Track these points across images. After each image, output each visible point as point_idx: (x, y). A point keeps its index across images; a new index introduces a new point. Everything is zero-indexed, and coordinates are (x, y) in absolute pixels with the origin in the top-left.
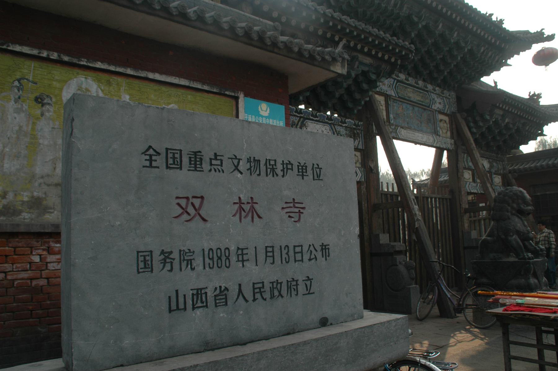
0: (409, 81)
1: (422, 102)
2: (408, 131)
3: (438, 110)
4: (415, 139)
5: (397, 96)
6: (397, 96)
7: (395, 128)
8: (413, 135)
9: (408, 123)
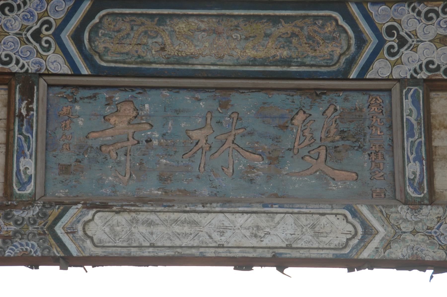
1: (287, 62)
2: (142, 217)
3: (424, 75)
4: (198, 247)
5: (85, 70)
6: (85, 70)
7: (45, 215)
8: (186, 229)
9: (162, 178)
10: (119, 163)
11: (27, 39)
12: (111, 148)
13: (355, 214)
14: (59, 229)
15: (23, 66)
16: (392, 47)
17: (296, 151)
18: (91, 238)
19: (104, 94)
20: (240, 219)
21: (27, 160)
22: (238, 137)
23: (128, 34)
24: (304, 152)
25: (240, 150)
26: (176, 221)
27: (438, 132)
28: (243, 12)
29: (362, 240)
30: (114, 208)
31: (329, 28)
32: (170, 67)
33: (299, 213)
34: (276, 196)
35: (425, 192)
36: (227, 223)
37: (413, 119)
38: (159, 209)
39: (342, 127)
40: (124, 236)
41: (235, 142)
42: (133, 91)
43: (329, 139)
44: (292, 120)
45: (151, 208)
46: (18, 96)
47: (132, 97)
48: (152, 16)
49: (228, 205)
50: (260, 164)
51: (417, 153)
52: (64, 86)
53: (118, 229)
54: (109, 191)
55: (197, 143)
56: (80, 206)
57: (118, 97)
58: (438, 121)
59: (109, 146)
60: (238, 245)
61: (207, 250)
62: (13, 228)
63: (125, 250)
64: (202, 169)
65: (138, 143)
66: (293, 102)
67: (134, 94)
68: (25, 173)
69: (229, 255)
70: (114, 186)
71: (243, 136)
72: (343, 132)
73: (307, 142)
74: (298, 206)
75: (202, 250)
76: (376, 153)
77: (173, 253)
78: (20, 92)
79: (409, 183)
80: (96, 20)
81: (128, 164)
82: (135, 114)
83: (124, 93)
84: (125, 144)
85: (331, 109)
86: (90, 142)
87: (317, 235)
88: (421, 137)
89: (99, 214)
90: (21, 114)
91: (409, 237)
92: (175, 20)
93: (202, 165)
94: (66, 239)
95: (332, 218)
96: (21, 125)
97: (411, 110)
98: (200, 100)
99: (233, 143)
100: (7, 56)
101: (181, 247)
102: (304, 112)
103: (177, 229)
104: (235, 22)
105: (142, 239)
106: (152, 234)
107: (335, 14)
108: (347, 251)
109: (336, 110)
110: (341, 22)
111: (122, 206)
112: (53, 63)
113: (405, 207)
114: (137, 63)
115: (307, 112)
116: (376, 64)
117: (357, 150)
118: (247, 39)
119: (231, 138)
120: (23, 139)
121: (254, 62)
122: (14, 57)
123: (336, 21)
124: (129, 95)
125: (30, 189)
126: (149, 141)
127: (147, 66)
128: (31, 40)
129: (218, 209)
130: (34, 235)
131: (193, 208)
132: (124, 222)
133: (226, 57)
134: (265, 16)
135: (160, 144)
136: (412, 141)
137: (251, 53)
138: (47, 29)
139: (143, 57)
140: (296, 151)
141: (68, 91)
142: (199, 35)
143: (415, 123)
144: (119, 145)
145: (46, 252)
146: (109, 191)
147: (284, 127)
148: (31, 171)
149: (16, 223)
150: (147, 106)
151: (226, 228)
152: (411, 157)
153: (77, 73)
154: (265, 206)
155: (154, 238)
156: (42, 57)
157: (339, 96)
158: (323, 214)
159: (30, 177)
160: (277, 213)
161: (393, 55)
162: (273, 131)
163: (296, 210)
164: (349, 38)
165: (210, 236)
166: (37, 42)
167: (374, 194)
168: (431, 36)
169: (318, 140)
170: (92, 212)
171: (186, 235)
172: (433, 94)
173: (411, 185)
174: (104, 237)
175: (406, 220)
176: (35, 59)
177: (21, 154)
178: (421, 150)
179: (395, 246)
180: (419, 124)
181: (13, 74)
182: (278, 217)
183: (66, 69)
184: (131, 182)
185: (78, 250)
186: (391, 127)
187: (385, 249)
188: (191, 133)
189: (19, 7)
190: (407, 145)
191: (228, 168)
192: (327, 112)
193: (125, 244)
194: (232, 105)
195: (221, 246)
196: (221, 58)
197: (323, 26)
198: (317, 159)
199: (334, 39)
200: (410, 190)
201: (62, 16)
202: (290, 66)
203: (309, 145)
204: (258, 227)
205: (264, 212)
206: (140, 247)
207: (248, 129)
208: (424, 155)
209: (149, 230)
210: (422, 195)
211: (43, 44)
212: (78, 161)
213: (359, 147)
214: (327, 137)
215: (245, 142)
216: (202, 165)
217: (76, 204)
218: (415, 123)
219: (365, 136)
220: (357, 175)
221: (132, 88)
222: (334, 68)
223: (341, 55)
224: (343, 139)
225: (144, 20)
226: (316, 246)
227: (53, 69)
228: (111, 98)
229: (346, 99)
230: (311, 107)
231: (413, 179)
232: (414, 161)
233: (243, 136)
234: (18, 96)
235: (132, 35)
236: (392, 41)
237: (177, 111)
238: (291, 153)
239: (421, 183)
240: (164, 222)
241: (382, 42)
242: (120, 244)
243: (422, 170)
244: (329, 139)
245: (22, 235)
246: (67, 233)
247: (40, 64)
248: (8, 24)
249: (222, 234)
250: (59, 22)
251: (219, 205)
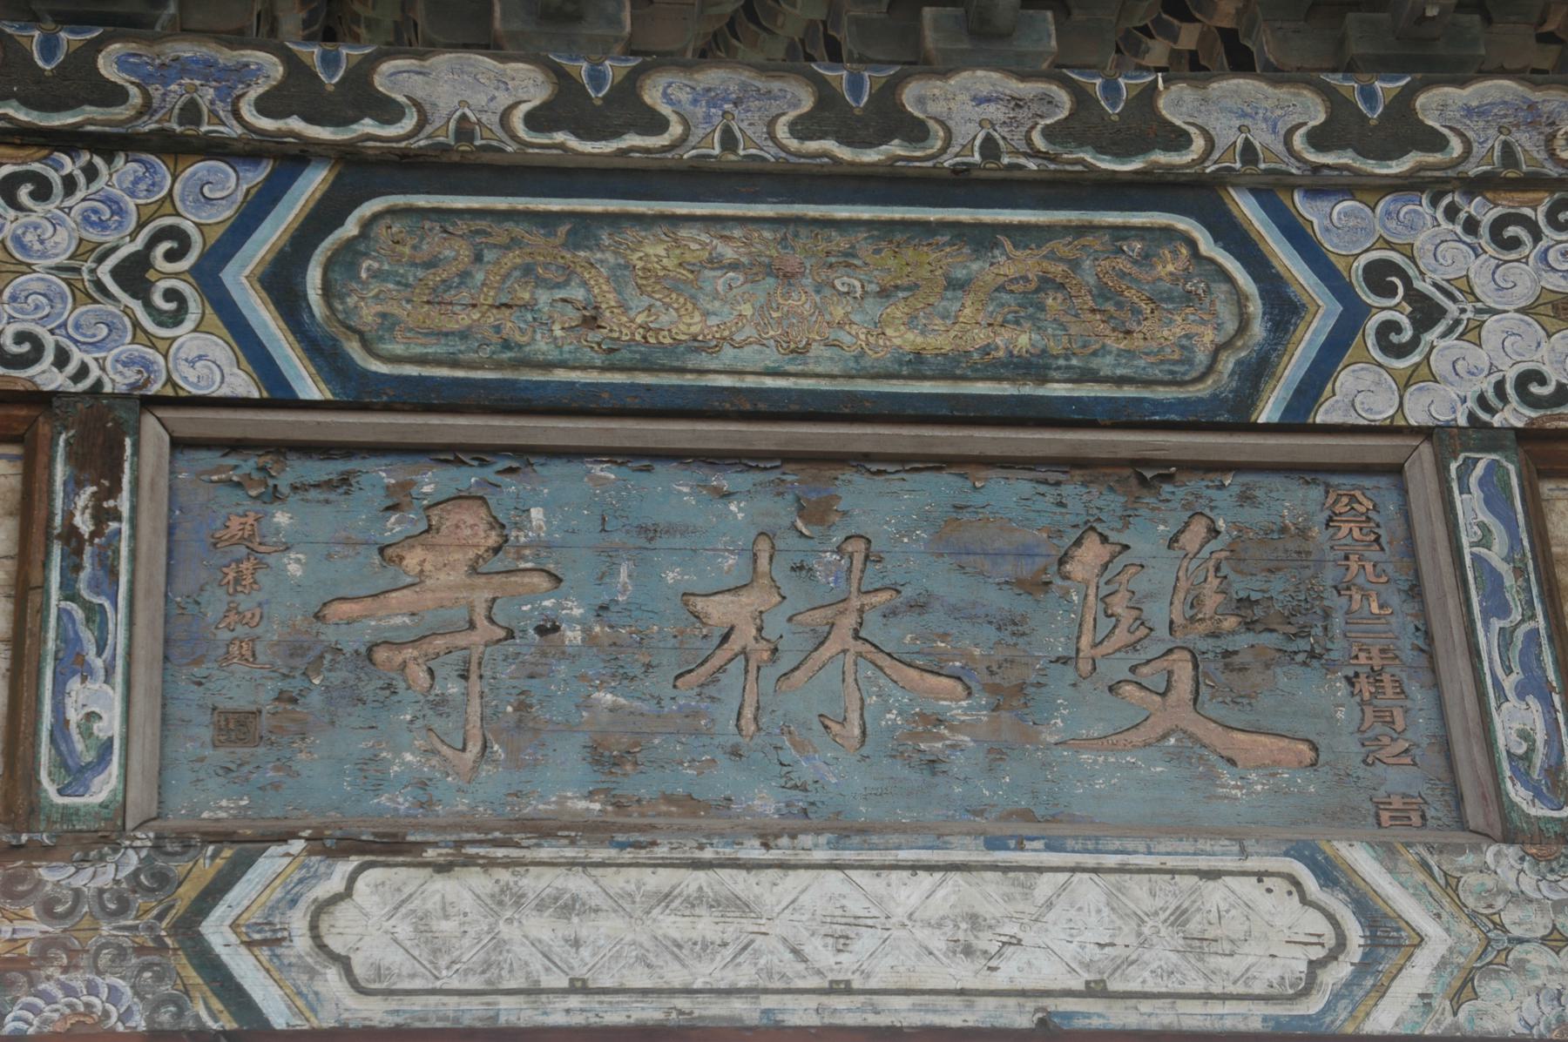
0: (658, 124)
1: (1033, 367)
2: (535, 883)
3: (1514, 415)
4: (753, 992)
5: (309, 387)
6: (309, 387)
7: (163, 880)
8: (706, 926)
10: (440, 704)
11: (100, 286)
12: (409, 652)
13: (1329, 873)
14: (216, 931)
15: (83, 371)
16: (1389, 327)
17: (1085, 667)
18: (344, 963)
19: (381, 474)
20: (903, 893)
21: (96, 685)
22: (870, 617)
23: (465, 275)
24: (1118, 669)
25: (885, 662)
26: (665, 898)
28: (865, 213)
29: (1366, 966)
30: (430, 854)
31: (1169, 266)
33: (1122, 870)
34: (1027, 816)
36: (856, 906)
37: (1495, 556)
38: (599, 854)
39: (1242, 586)
40: (470, 953)
41: (862, 634)
42: (483, 463)
44: (1062, 562)
45: (570, 853)
46: (60, 471)
48: (547, 220)
49: (856, 840)
50: (958, 709)
53: (447, 926)
54: (403, 803)
55: (725, 638)
56: (297, 846)
57: (431, 482)
60: (904, 983)
62: (36, 928)
64: (749, 726)
65: (510, 635)
66: (1061, 504)
67: (489, 473)
68: (87, 733)
69: (873, 1020)
70: (423, 785)
71: (890, 613)
72: (1245, 602)
73: (1121, 637)
74: (1117, 844)
75: (768, 1002)
78: (70, 457)
79: (1514, 769)
80: (350, 228)
81: (475, 708)
82: (493, 539)
83: (453, 471)
84: (461, 640)
85: (1199, 528)
86: (330, 635)
87: (1197, 946)
88: (1533, 617)
90: (71, 532)
91: (1539, 958)
92: (631, 234)
93: (748, 713)
94: (245, 968)
95: (1247, 886)
96: (72, 568)
97: (1483, 526)
98: (727, 496)
99: (857, 637)
100: (20, 338)
101: (688, 991)
102: (1104, 539)
103: (670, 925)
104: (840, 242)
105: (537, 964)
106: (576, 943)
107: (1183, 224)
108: (1312, 1006)
109: (1214, 532)
110: (1207, 245)
111: (459, 844)
112: (192, 363)
113: (1512, 851)
114: (499, 366)
115: (1114, 537)
116: (1346, 380)
117: (1304, 664)
118: (884, 293)
119: (850, 621)
120: (79, 614)
121: (916, 364)
122: (49, 341)
123: (1192, 244)
124: (469, 477)
125: (103, 789)
127: (537, 376)
129: (820, 856)
130: (121, 953)
131: (728, 852)
132: (467, 902)
133: (817, 349)
134: (943, 225)
135: (590, 639)
137: (905, 339)
138: (171, 256)
139: (520, 346)
140: (1085, 667)
141: (248, 464)
142: (720, 281)
143: (1504, 568)
144: (440, 642)
145: (165, 1017)
147: (1037, 586)
148: (111, 725)
149: (48, 911)
150: (536, 514)
151: (856, 922)
152: (1509, 683)
153: (281, 398)
154: (993, 844)
155: (582, 964)
156: (152, 342)
157: (1222, 487)
158: (1212, 875)
159: (106, 748)
160: (1040, 870)
161: (1401, 351)
162: (1000, 600)
163: (1111, 860)
164: (1240, 299)
166: (134, 296)
167: (1385, 816)
168: (1524, 292)
169: (1162, 631)
170: (344, 868)
171: (705, 948)
172: (1547, 488)
173: (1522, 776)
174: (394, 958)
175: (1518, 898)
176: (127, 348)
177: (73, 664)
179: (1489, 988)
180: (1520, 572)
181: (42, 400)
182: (1046, 885)
183: (242, 384)
184: (486, 770)
186: (1415, 591)
187: (1457, 999)
188: (700, 604)
189: (70, 184)
190: (1487, 641)
191: (843, 722)
192: (1183, 538)
193: (474, 983)
194: (845, 513)
196: (800, 352)
197: (1146, 259)
198: (1163, 695)
199: (1189, 298)
201: (227, 213)
202: (1043, 380)
203: (1133, 646)
204: (974, 920)
205: (994, 867)
206: (533, 991)
207: (908, 592)
208: (1552, 676)
209: (565, 929)
211: (158, 300)
213: (1312, 655)
214: (1192, 619)
215: (902, 634)
216: (748, 713)
217: (283, 838)
218: (1504, 568)
219: (1327, 614)
220: (1315, 748)
221: (481, 453)
222: (1202, 390)
223: (1218, 349)
224: (1249, 625)
225: (518, 230)
226: (1198, 986)
227: (193, 381)
228: (405, 486)
229: (1246, 498)
230: (1126, 520)
231: (1527, 757)
233: (890, 613)
234: (60, 471)
235: (480, 276)
236: (1391, 310)
237: (650, 532)
238: (1070, 674)
240: (620, 903)
241: (1354, 316)
242: (455, 984)
245: (71, 952)
246: (250, 944)
247: (146, 365)
248: (30, 238)
249: (842, 943)
250: (214, 235)
251: (822, 840)
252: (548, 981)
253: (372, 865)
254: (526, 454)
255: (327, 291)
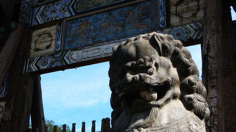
2: (85, 50)
4: (100, 55)
5: (74, 15)
7: (62, 55)
8: (97, 51)
10: (82, 37)
11: (61, 10)
12: (81, 33)
14: (65, 58)
17: (130, 22)
18: (73, 59)
20: (111, 45)
21: (59, 41)
22: (114, 22)
23: (85, 2)
24: (132, 22)
25: (114, 26)
26: (94, 49)
27: (171, 7)
30: (79, 49)
32: (95, 7)
35: (165, 25)
37: (162, 5)
39: (143, 12)
40: (81, 56)
41: (113, 24)
42: (87, 17)
43: (139, 17)
44: (129, 14)
45: (88, 47)
47: (87, 18)
49: (108, 42)
51: (163, 14)
52: (70, 20)
54: (79, 45)
55: (103, 27)
56: (70, 50)
58: (172, 4)
59: (80, 33)
60: (111, 52)
61: (102, 56)
63: (81, 60)
64: (104, 34)
65: (88, 30)
66: (129, 9)
67: (87, 18)
68: (58, 45)
69: (108, 56)
71: (115, 22)
72: (143, 14)
73: (133, 19)
74: (128, 37)
75: (101, 56)
76: (153, 17)
77: (93, 58)
79: (161, 23)
83: (85, 18)
84: (84, 32)
85: (140, 8)
86: (76, 33)
88: (164, 9)
89: (75, 52)
93: (104, 33)
94: (67, 60)
97: (162, 2)
98: (104, 15)
99: (112, 24)
101: (95, 56)
102: (133, 11)
103: (94, 51)
105: (85, 56)
106: (88, 54)
111: (81, 48)
112: (66, 15)
114: (87, 9)
115: (133, 10)
117: (147, 18)
120: (58, 36)
122: (58, 16)
126: (90, 29)
127: (89, 9)
128: (62, 10)
129: (105, 43)
131: (99, 45)
132: (81, 52)
135: (93, 29)
136: (162, 11)
139: (88, 7)
140: (130, 22)
141: (71, 21)
143: (162, 5)
144: (83, 32)
146: (79, 45)
147: (126, 17)
149: (55, 59)
150: (90, 20)
151: (108, 48)
153: (72, 16)
154: (119, 39)
155: (88, 56)
156: (64, 14)
157: (143, 4)
160: (122, 41)
162: (123, 18)
165: (103, 52)
166: (63, 10)
167: (152, 30)
169: (136, 18)
173: (161, 24)
174: (76, 58)
178: (164, 13)
180: (164, 5)
184: (85, 42)
185: (69, 62)
188: (101, 25)
189: (60, 3)
191: (111, 32)
192: (139, 9)
194: (113, 14)
195: (106, 54)
198: (136, 23)
200: (161, 25)
203: (134, 20)
205: (118, 41)
207: (117, 20)
208: (165, 14)
209: (87, 53)
210: (164, 26)
211: (65, 10)
212: (72, 39)
213: (148, 17)
214: (139, 16)
215: (116, 23)
216: (104, 33)
218: (162, 5)
219: (150, 13)
220: (147, 25)
224: (143, 16)
227: (66, 16)
228: (82, 20)
229: (145, 4)
230: (134, 9)
231: (162, 22)
232: (162, 17)
233: (115, 22)
235: (86, 2)
237: (98, 19)
238: (128, 23)
239: (164, 22)
240: (91, 50)
242: (80, 59)
243: (164, 18)
244: (139, 17)
245: (56, 61)
246: (67, 58)
247: (64, 16)
248: (57, 8)
249: (106, 50)
250: (69, 4)
251: (106, 42)
252: (86, 57)
253: (75, 51)
254: (90, 16)
255: (76, 7)
